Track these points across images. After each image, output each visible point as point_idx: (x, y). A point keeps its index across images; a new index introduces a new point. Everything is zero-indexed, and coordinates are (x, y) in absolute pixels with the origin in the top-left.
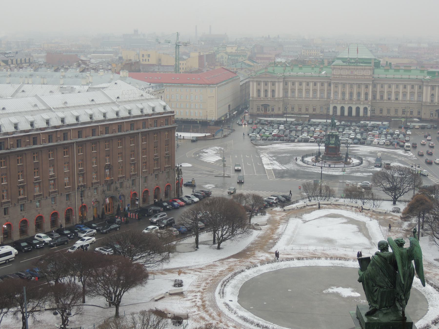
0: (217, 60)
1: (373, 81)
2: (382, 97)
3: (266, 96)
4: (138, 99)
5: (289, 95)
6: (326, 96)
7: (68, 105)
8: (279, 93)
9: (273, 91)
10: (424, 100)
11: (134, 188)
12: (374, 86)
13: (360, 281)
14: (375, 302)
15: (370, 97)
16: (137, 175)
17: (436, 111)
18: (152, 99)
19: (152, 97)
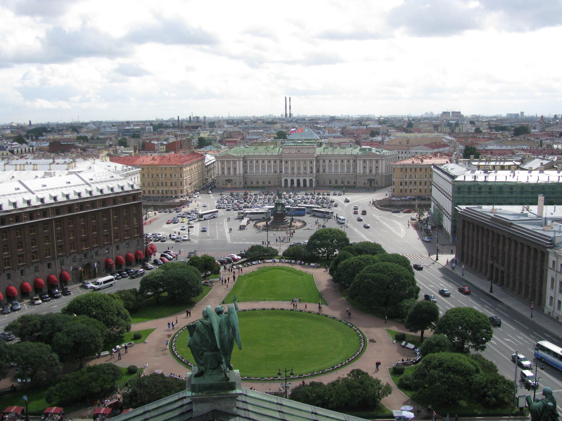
0: (192, 144)
1: (316, 157)
3: (229, 173)
4: (109, 179)
5: (249, 172)
8: (240, 170)
10: (358, 172)
12: (318, 161)
13: (189, 346)
14: (202, 365)
15: (314, 171)
16: (111, 244)
17: (368, 180)
18: (121, 179)
19: (122, 178)
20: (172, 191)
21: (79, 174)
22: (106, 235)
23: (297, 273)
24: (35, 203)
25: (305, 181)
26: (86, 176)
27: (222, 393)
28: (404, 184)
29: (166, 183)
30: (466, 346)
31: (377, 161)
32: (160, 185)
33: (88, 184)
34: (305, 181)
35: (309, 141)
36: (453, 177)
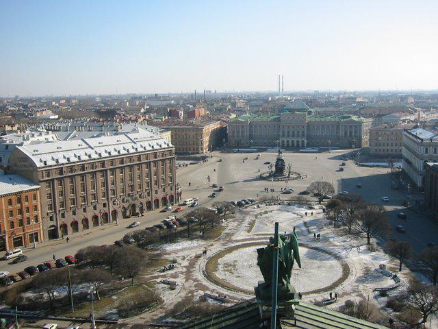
24: (94, 156)
33: (134, 143)
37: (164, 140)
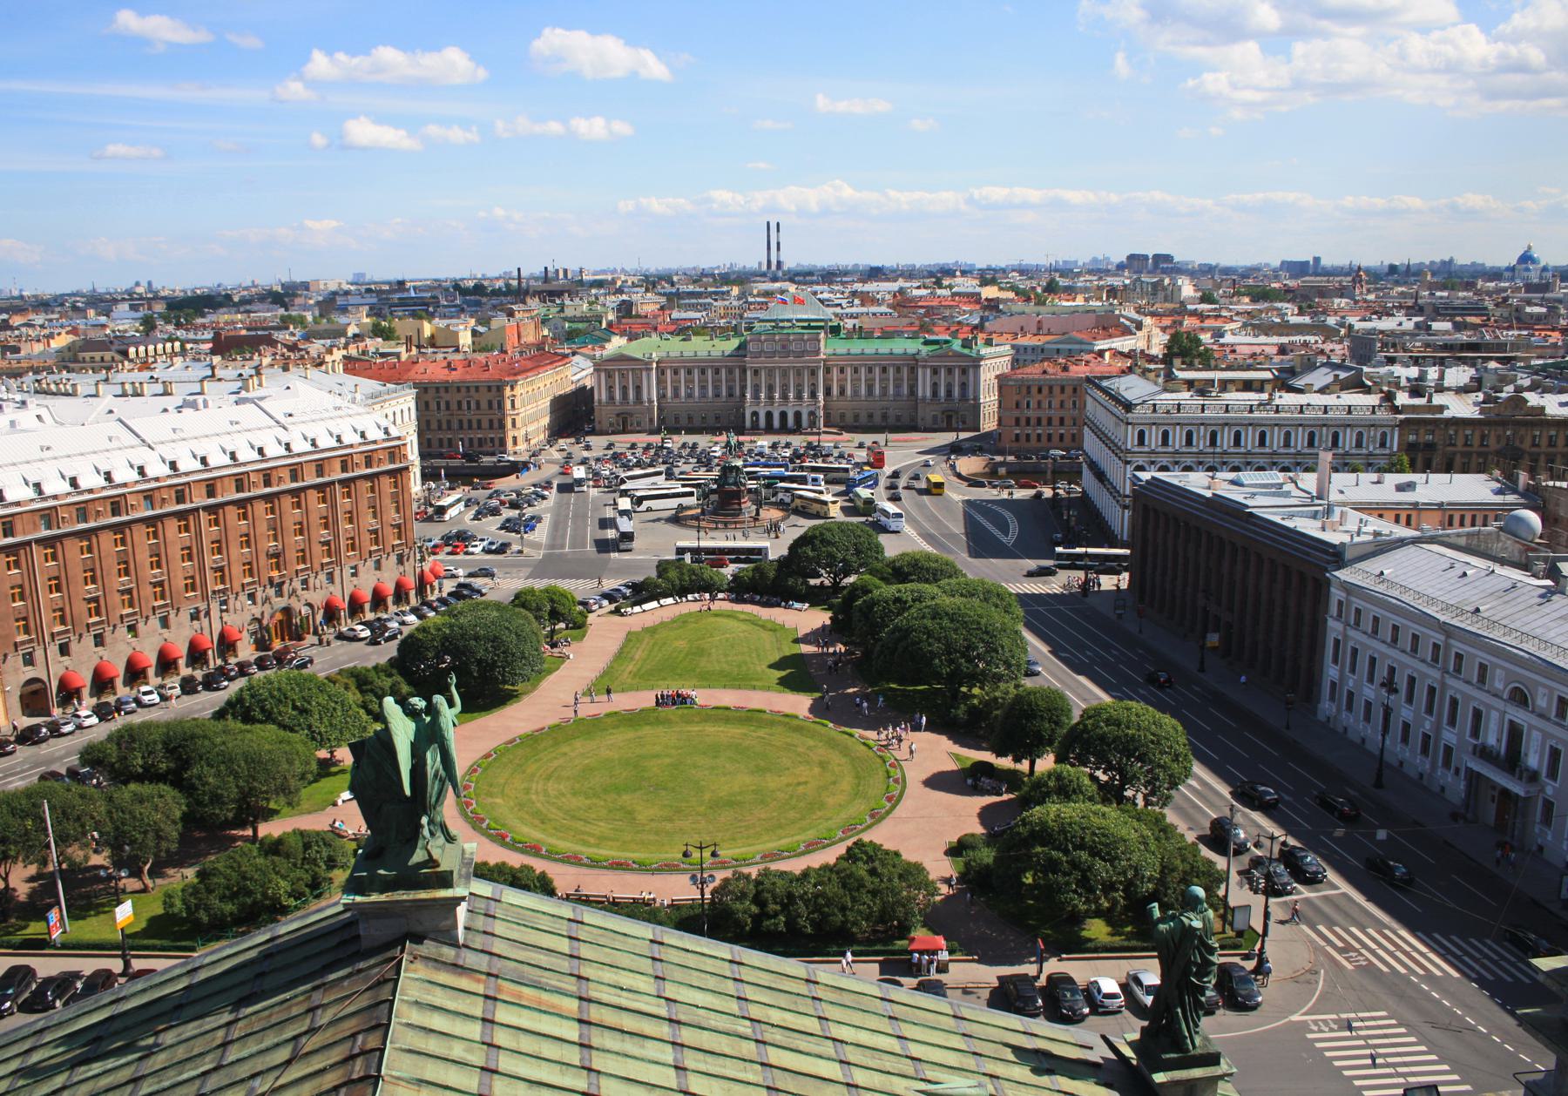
2: (842, 392)
6: (738, 393)
7: (183, 435)
8: (652, 392)
9: (638, 389)
10: (920, 394)
11: (332, 588)
12: (828, 370)
19: (361, 410)
20: (492, 440)
21: (261, 403)
22: (327, 543)
23: (763, 627)
24: (157, 469)
25: (798, 415)
26: (276, 407)
27: (423, 895)
28: (1023, 422)
29: (479, 422)
30: (1129, 793)
31: (964, 371)
32: (466, 425)
34: (798, 415)
35: (809, 325)
36: (1129, 407)
37: (394, 417)
